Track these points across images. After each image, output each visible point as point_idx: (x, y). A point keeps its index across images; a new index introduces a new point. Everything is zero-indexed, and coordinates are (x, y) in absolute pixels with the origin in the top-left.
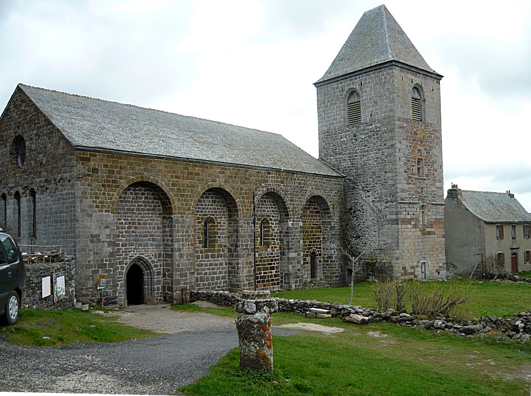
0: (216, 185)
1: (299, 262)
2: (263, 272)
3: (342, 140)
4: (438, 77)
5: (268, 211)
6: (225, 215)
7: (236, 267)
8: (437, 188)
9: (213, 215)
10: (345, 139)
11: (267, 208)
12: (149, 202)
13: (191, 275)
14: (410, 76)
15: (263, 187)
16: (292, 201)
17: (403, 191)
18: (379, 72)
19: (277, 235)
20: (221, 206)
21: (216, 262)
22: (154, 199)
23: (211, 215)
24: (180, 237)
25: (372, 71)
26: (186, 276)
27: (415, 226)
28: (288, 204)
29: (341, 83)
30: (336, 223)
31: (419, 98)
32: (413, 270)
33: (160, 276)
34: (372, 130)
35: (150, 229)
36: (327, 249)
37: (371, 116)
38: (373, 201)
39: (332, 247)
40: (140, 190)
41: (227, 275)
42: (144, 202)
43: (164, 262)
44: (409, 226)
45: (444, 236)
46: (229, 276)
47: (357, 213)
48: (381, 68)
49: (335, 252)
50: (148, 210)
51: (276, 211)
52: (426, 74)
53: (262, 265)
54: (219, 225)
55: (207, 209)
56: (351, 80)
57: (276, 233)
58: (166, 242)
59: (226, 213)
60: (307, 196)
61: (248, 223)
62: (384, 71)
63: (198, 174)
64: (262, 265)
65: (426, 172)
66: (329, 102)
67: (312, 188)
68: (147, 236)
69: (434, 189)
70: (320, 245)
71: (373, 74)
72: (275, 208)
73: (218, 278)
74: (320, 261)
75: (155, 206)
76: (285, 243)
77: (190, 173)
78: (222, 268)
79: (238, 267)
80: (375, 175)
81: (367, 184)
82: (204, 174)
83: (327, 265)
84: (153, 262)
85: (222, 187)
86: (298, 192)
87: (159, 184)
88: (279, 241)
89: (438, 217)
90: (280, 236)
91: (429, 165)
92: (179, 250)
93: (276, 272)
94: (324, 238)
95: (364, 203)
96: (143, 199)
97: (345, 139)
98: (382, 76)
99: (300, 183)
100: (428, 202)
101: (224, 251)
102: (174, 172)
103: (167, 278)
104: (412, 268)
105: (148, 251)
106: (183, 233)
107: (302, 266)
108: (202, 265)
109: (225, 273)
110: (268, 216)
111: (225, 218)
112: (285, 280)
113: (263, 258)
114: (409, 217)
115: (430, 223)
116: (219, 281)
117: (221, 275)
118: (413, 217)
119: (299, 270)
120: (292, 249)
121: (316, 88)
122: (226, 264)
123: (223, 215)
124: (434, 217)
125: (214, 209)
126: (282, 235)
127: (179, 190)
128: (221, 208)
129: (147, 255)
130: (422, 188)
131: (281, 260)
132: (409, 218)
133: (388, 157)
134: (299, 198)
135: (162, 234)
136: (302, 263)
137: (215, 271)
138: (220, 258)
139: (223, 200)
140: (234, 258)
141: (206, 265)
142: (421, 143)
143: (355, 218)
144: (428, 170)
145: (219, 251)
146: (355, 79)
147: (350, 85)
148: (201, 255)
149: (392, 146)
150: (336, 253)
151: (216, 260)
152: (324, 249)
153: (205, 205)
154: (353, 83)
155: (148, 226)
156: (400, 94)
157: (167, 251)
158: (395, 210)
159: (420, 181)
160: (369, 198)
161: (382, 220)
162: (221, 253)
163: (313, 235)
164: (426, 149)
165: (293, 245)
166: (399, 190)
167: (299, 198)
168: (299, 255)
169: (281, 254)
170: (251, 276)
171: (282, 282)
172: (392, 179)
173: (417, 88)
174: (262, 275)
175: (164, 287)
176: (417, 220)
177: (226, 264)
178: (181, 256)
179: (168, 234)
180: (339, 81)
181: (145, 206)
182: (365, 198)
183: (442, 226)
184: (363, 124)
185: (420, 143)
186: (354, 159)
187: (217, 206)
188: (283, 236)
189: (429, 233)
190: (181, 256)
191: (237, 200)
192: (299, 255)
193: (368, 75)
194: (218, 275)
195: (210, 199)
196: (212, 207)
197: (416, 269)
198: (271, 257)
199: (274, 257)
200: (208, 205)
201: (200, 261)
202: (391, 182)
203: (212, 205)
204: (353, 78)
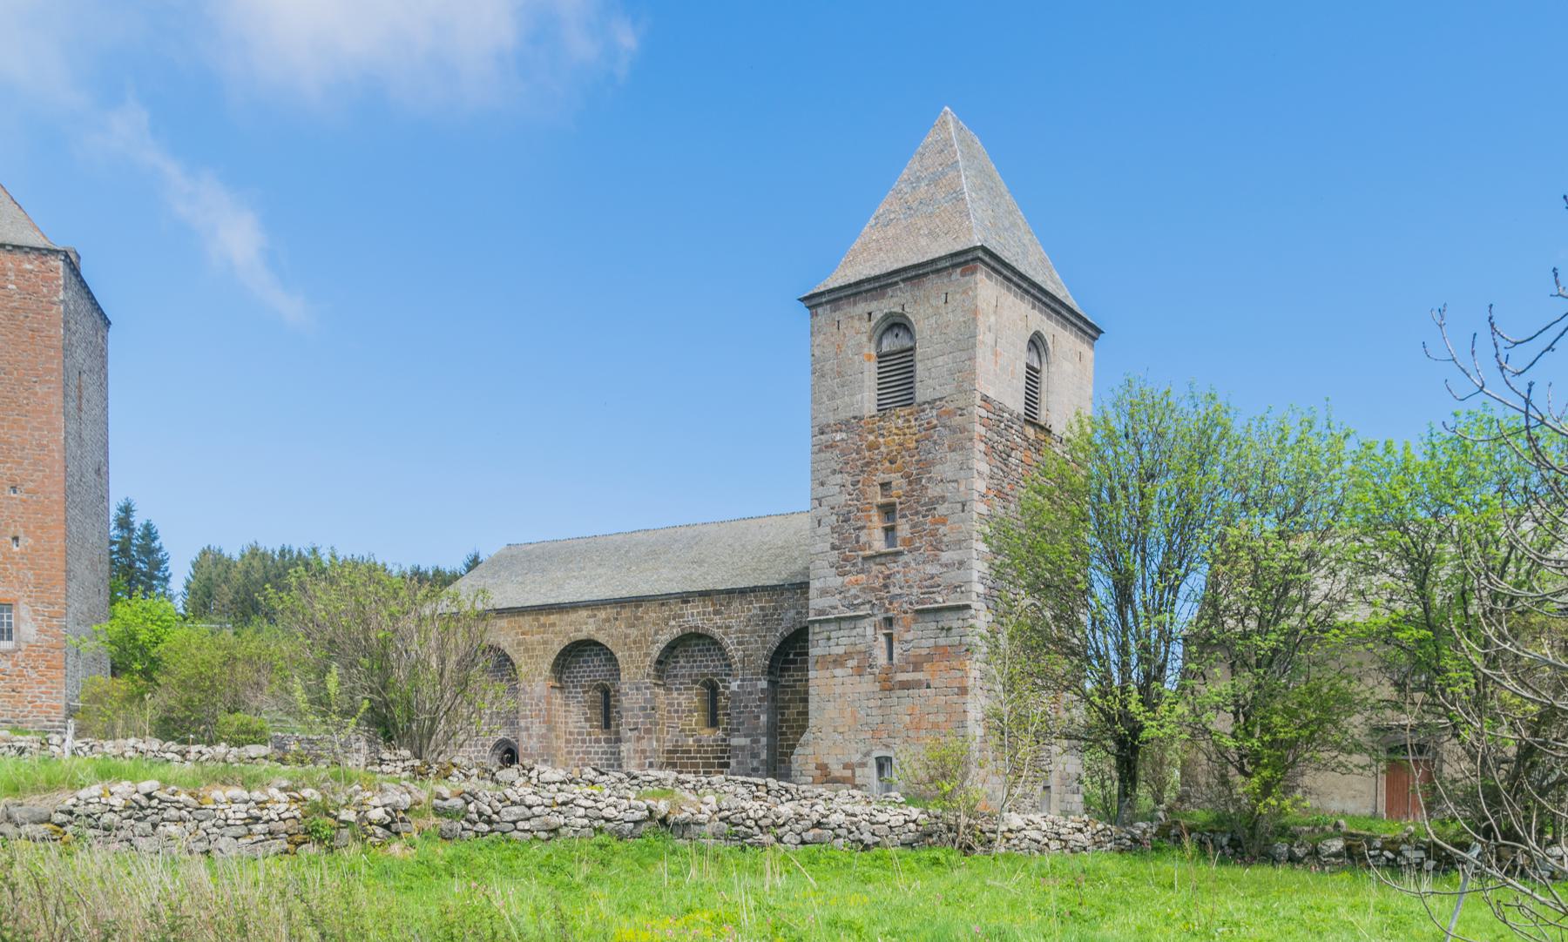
16: (739, 643)
17: (824, 592)
27: (859, 671)
32: (848, 773)
63: (553, 625)
77: (544, 625)
92: (527, 729)
99: (762, 609)
110: (717, 675)
114: (840, 650)
118: (850, 649)
127: (526, 650)
176: (868, 654)
178: (530, 736)
190: (530, 736)
191: (618, 655)
192: (756, 741)
197: (858, 771)
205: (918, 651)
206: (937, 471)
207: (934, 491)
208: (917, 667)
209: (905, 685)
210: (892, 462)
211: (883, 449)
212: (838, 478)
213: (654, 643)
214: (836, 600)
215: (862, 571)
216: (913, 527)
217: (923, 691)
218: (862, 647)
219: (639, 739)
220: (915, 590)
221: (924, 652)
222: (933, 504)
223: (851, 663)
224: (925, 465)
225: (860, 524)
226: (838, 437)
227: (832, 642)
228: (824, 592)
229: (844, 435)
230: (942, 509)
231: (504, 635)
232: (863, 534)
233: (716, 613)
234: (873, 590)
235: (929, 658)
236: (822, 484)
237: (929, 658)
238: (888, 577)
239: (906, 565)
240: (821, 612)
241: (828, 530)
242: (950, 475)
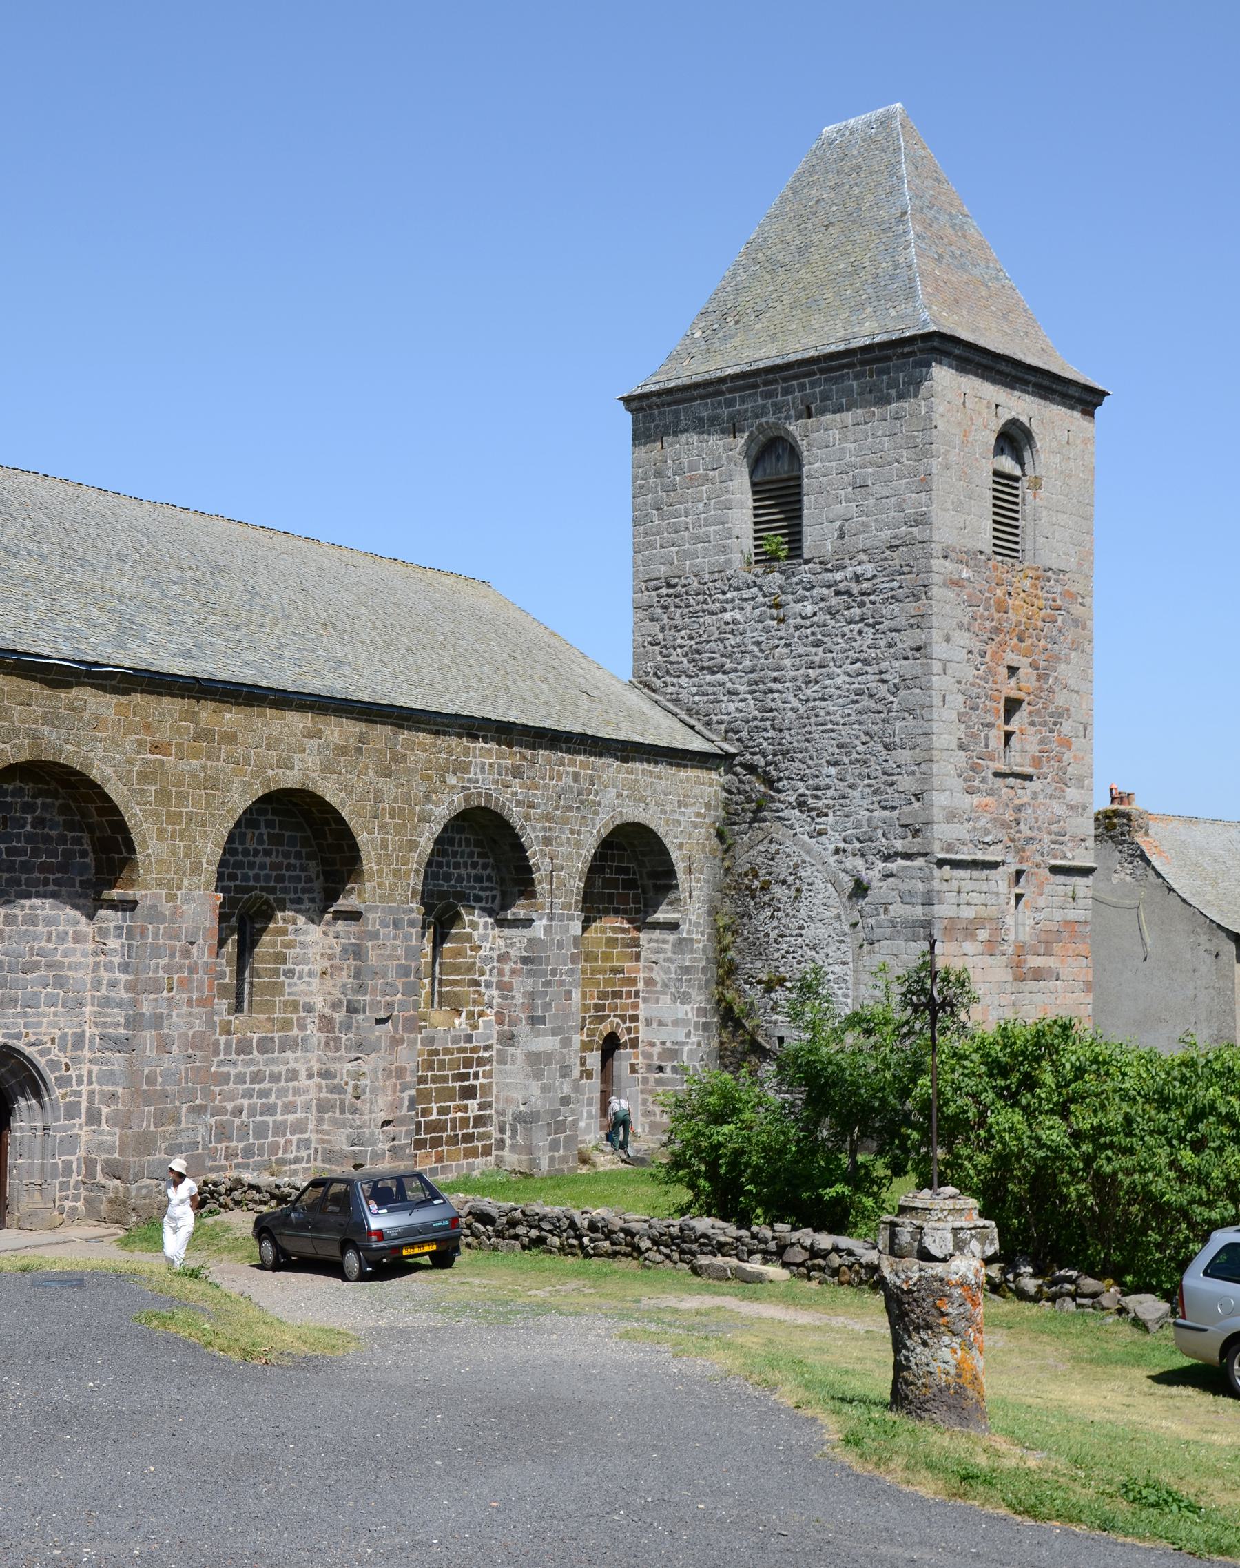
0: (291, 779)
1: (565, 1072)
2: (434, 1106)
3: (727, 616)
4: (1089, 398)
5: (460, 879)
6: (310, 890)
7: (350, 1089)
8: (1071, 807)
9: (272, 890)
10: (737, 615)
11: (457, 866)
12: (47, 839)
13: (193, 1117)
14: (992, 392)
15: (454, 787)
17: (952, 816)
18: (880, 372)
19: (487, 968)
20: (298, 856)
21: (276, 1069)
22: (69, 825)
23: (262, 889)
24: (161, 974)
25: (850, 366)
26: (178, 1121)
27: (991, 947)
28: (535, 854)
29: (730, 403)
30: (697, 925)
31: (1017, 472)
33: (77, 1121)
34: (842, 587)
35: (49, 940)
36: (660, 1023)
37: (841, 536)
38: (837, 851)
39: (681, 1015)
40: (18, 792)
41: (312, 1117)
42: (30, 838)
43: (96, 1068)
44: (968, 947)
45: (1088, 987)
46: (320, 1121)
47: (778, 890)
48: (888, 358)
49: (688, 1035)
50: (44, 868)
51: (489, 879)
52: (1046, 383)
53: (435, 1079)
54: (290, 927)
55: (251, 866)
56: (767, 395)
57: (486, 960)
58: (104, 991)
59: (317, 885)
60: (601, 825)
61: (396, 925)
62: (899, 369)
63: (230, 738)
64: (435, 1079)
65: (1033, 748)
66: (679, 471)
67: (619, 795)
68: (35, 967)
69: (1059, 809)
70: (635, 1006)
71: (856, 377)
72: (485, 867)
73: (280, 1129)
74: (633, 1069)
75: (68, 854)
76: (519, 1000)
77: (204, 735)
78: (297, 1092)
79: (356, 1087)
80: (848, 754)
81: (817, 788)
82: (251, 739)
83: (659, 1082)
84: (54, 1065)
85: (311, 787)
86: (570, 808)
87: (95, 775)
88: (495, 993)
89: (1072, 914)
90: (501, 973)
91: (1045, 724)
93: (482, 1107)
94: (649, 982)
95: (808, 859)
96: (28, 828)
97: (737, 615)
98: (890, 386)
99: (576, 777)
100: (1038, 858)
101: (303, 1027)
102: (148, 727)
103: (104, 1126)
105: (38, 1024)
106: (172, 956)
107: (576, 1087)
108: (225, 1079)
109: (307, 1108)
111: (312, 900)
112: (513, 1137)
113: (437, 1053)
114: (968, 913)
115: (1043, 937)
116: (282, 1141)
117: (291, 1117)
118: (984, 913)
119: (565, 1101)
120: (542, 1020)
121: (629, 416)
122: (310, 1076)
123: (304, 891)
124: (1058, 915)
125: (276, 866)
126: (507, 968)
127: (164, 796)
128: (298, 863)
129: (32, 1038)
130: (1019, 809)
131: (502, 1062)
132: (972, 915)
133: (902, 693)
134: (572, 832)
135: (90, 961)
136: (576, 1073)
137: (272, 1100)
138: (289, 1054)
139: (309, 833)
140: (342, 1053)
141: (240, 1079)
142: (1021, 640)
143: (768, 912)
144: (1042, 742)
145: (286, 1025)
146: (786, 392)
147: (764, 414)
148: (223, 1039)
149: (918, 649)
150: (694, 1039)
151: (273, 1061)
152: (648, 1023)
153: (246, 853)
154: (778, 408)
155: (40, 929)
156: (953, 457)
157: (109, 1025)
158: (920, 886)
159: (1011, 781)
160: (823, 838)
161: (872, 921)
162: (295, 1032)
163: (615, 971)
164: (1034, 666)
165: (546, 1007)
166: (938, 814)
167: (572, 832)
168: (566, 1043)
169: (500, 1041)
170: (403, 1121)
171: (501, 1144)
172: (913, 773)
173: (1013, 439)
174: (434, 1116)
175: (90, 1164)
177: (310, 1076)
178: (163, 1044)
179: (117, 960)
180: (722, 393)
181: (36, 853)
182: (806, 837)
183: (1081, 948)
184: (807, 562)
185: (1015, 640)
186: (771, 691)
187: (286, 855)
188: (513, 971)
189: (1038, 975)
190: (163, 1044)
191: (362, 838)
192: (566, 1043)
193: (835, 381)
194: (279, 1118)
195: (264, 831)
196: (268, 860)
198: (464, 1050)
199: (474, 1050)
200: (256, 853)
201: (221, 1063)
202: (906, 783)
203: (267, 853)
204: (779, 387)
213: (424, 819)
219: (395, 1042)
224: (1055, 658)
231: (103, 743)
233: (517, 772)
241: (954, 717)
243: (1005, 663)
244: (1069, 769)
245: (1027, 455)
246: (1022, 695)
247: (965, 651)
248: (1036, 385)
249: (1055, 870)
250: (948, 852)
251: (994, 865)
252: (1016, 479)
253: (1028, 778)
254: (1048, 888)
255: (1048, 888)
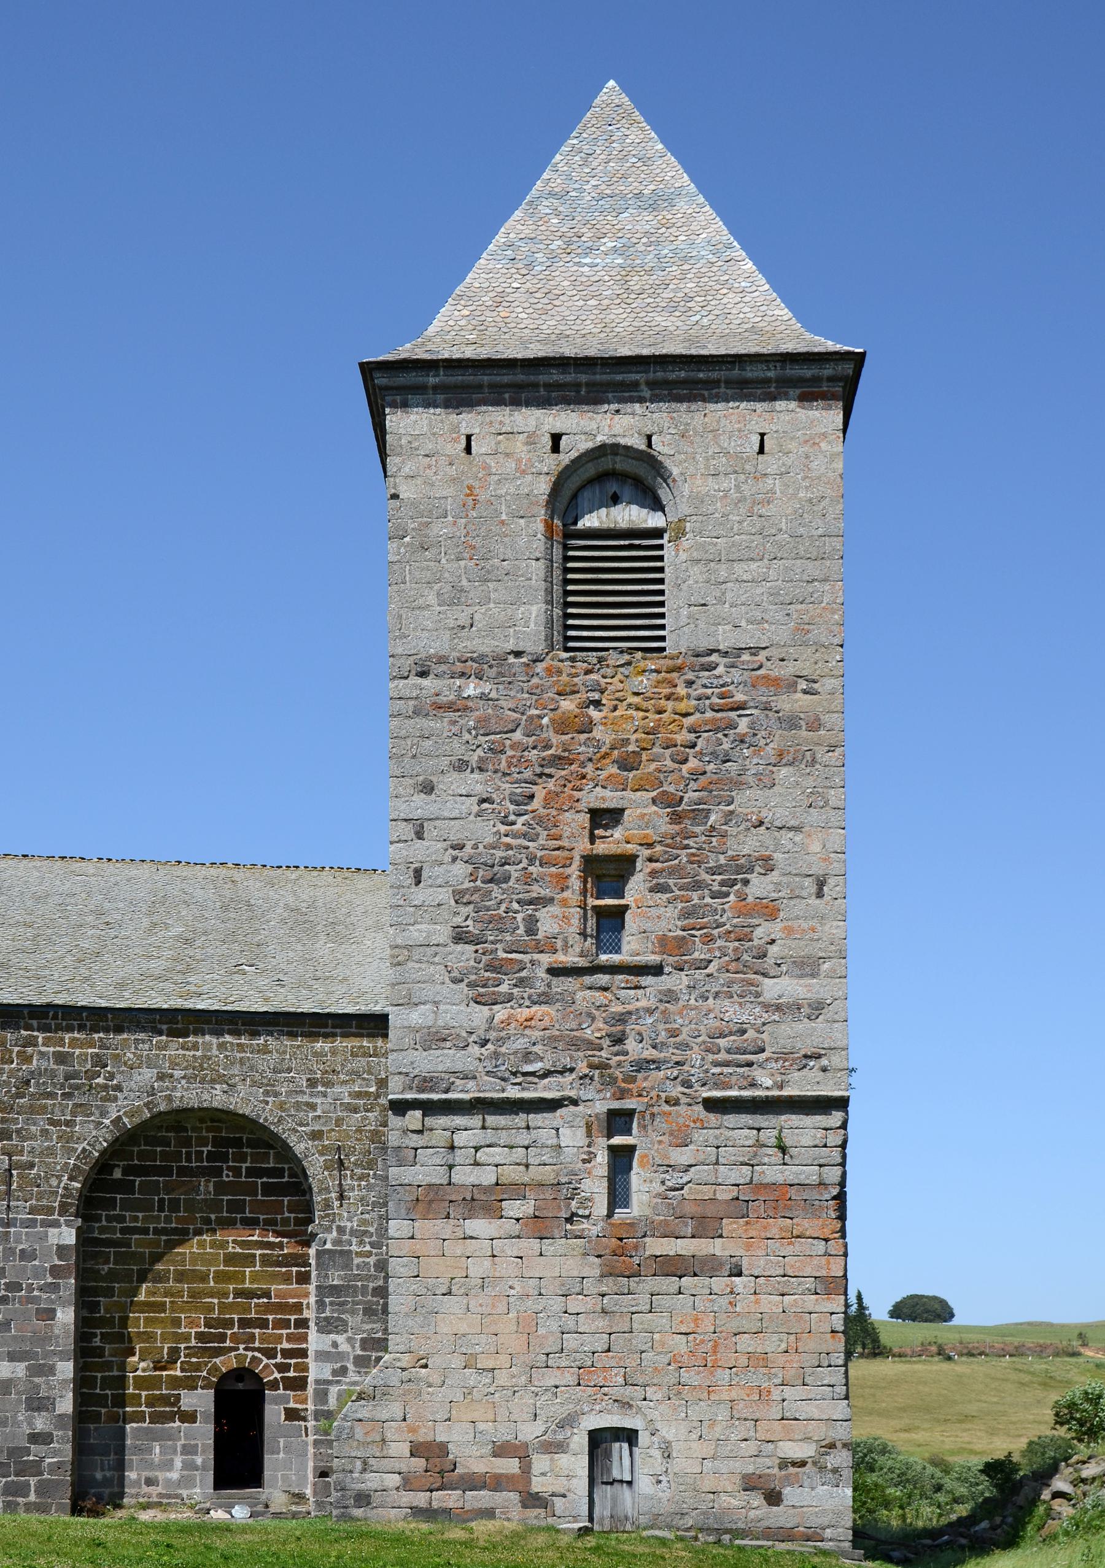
27: (539, 1226)
31: (655, 520)
32: (510, 1466)
104: (500, 1450)
114: (488, 1177)
176: (564, 1189)
197: (540, 1463)
205: (707, 1192)
206: (746, 801)
207: (748, 844)
208: (706, 1225)
209: (674, 1267)
210: (627, 764)
211: (598, 733)
212: (476, 783)
214: (469, 1058)
215: (544, 999)
216: (686, 914)
217: (719, 1283)
218: (547, 1174)
220: (695, 1056)
221: (725, 1194)
222: (738, 872)
223: (514, 1208)
225: (537, 891)
226: (472, 689)
227: (459, 1156)
228: (435, 1039)
229: (486, 687)
230: (759, 886)
232: (543, 914)
234: (575, 1044)
235: (740, 1207)
236: (428, 788)
237: (740, 1207)
238: (622, 1019)
239: (669, 996)
240: (427, 1083)
241: (444, 895)
242: (781, 815)
243: (582, 806)
244: (773, 950)
245: (664, 494)
246: (631, 848)
247: (475, 800)
248: (729, 383)
249: (711, 1105)
250: (421, 1090)
251: (552, 1105)
252: (658, 533)
253: (657, 970)
254: (699, 1136)
255: (699, 1136)
